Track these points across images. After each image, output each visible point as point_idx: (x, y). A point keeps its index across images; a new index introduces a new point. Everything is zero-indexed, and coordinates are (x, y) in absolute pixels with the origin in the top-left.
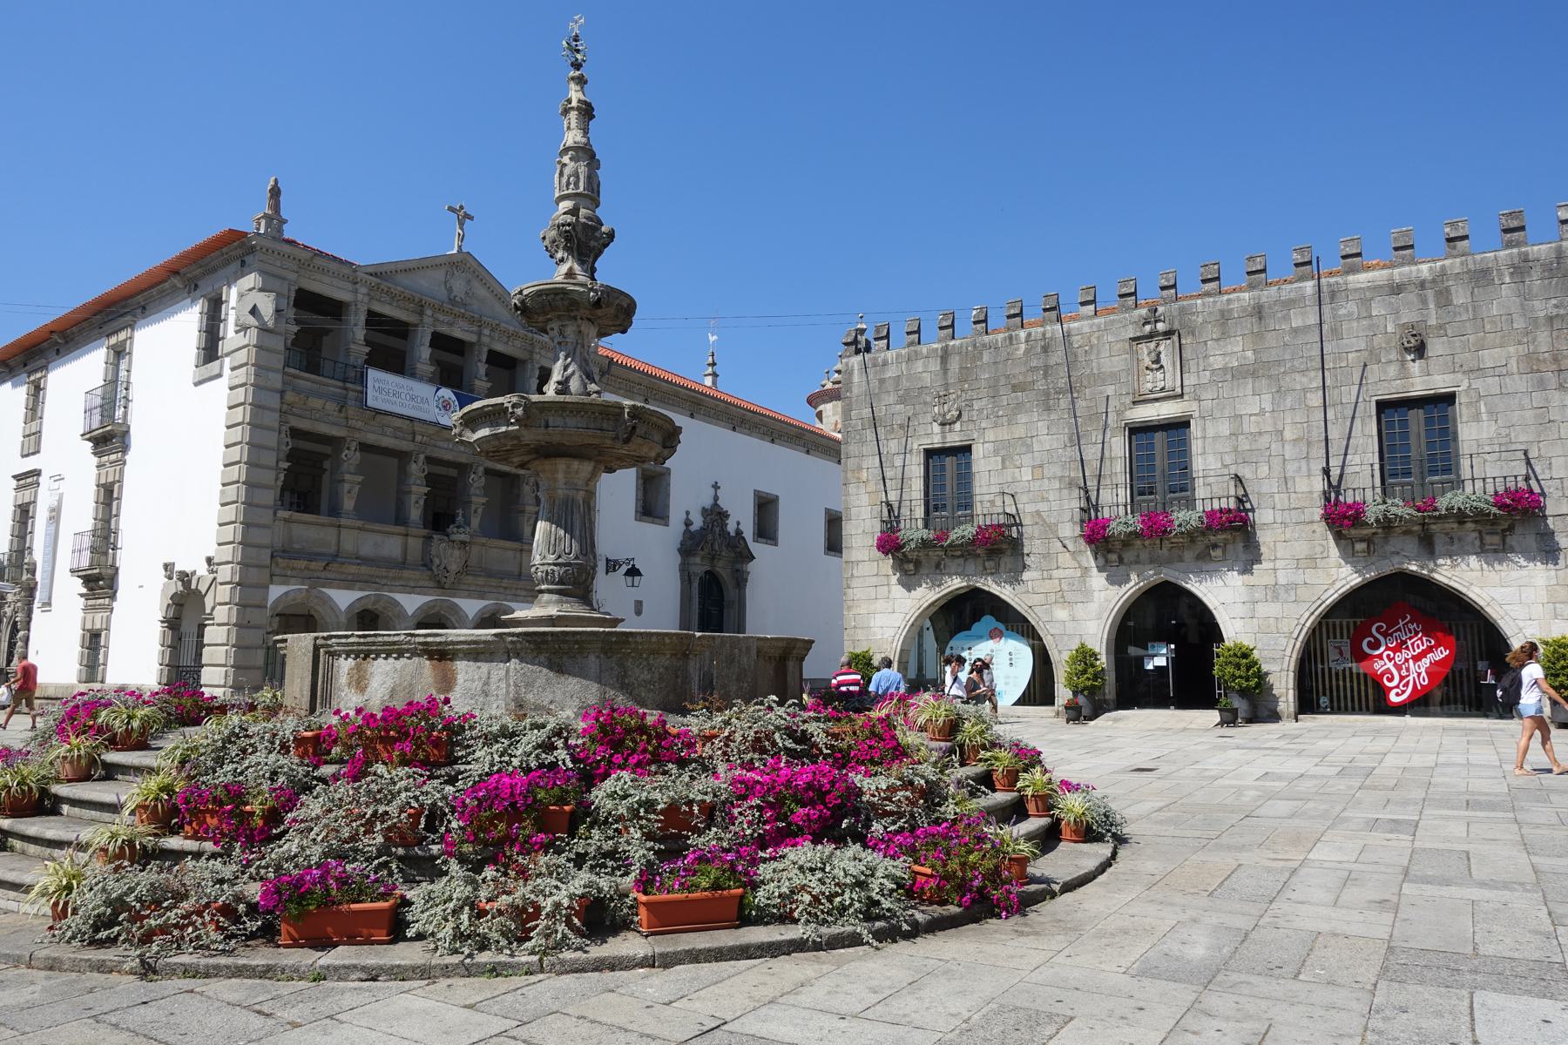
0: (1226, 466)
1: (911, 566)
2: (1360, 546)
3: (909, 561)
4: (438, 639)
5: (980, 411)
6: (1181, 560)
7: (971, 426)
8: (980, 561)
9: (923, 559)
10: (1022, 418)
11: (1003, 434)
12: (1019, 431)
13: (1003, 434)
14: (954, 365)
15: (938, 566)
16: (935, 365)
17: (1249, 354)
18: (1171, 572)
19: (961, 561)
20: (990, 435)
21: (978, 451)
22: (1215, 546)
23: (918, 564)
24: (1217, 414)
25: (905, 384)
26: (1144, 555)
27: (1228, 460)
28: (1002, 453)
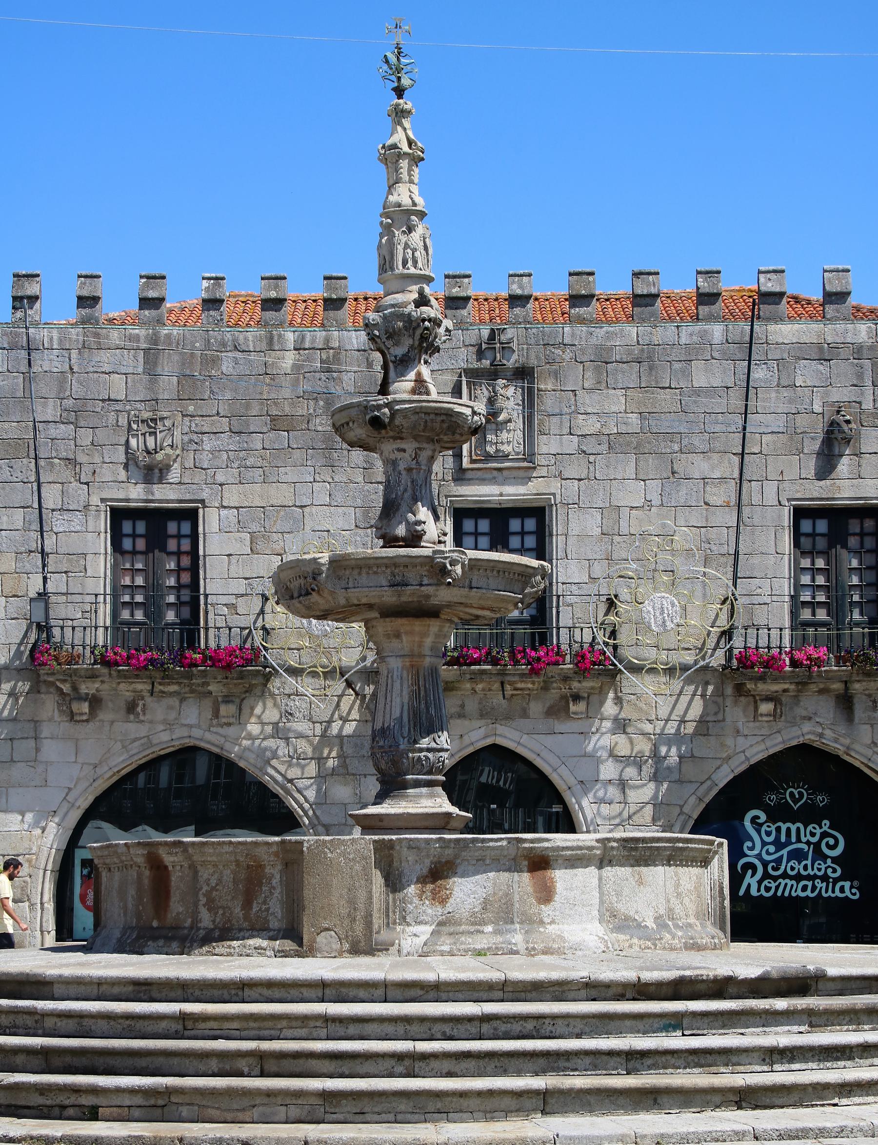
0: (593, 579)
1: (85, 707)
2: (766, 707)
3: (81, 698)
4: (546, 844)
5: (215, 452)
6: (525, 714)
7: (199, 477)
8: (208, 703)
9: (104, 694)
10: (290, 474)
11: (256, 494)
12: (281, 495)
13: (256, 494)
14: (168, 368)
15: (131, 708)
16: (135, 363)
17: (634, 418)
18: (514, 735)
19: (174, 701)
20: (232, 496)
21: (211, 522)
22: (576, 698)
23: (95, 702)
24: (585, 501)
25: (77, 390)
26: (472, 706)
27: (598, 570)
28: (254, 527)
